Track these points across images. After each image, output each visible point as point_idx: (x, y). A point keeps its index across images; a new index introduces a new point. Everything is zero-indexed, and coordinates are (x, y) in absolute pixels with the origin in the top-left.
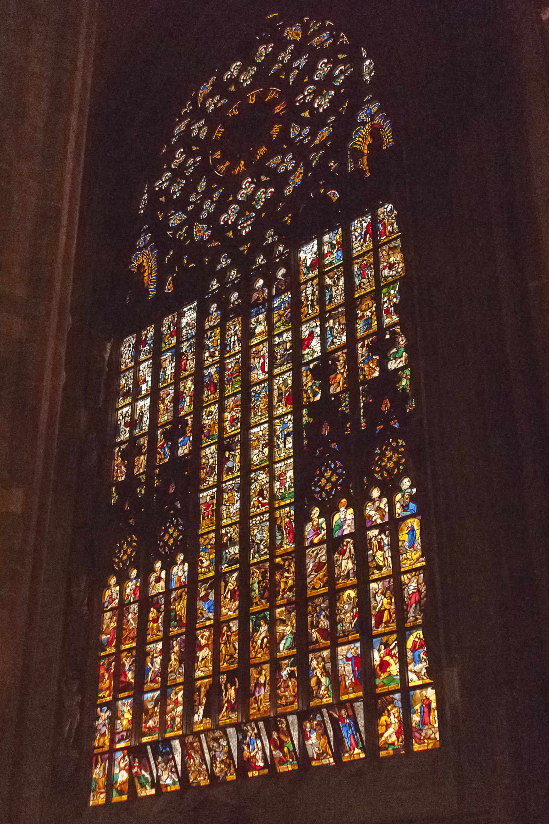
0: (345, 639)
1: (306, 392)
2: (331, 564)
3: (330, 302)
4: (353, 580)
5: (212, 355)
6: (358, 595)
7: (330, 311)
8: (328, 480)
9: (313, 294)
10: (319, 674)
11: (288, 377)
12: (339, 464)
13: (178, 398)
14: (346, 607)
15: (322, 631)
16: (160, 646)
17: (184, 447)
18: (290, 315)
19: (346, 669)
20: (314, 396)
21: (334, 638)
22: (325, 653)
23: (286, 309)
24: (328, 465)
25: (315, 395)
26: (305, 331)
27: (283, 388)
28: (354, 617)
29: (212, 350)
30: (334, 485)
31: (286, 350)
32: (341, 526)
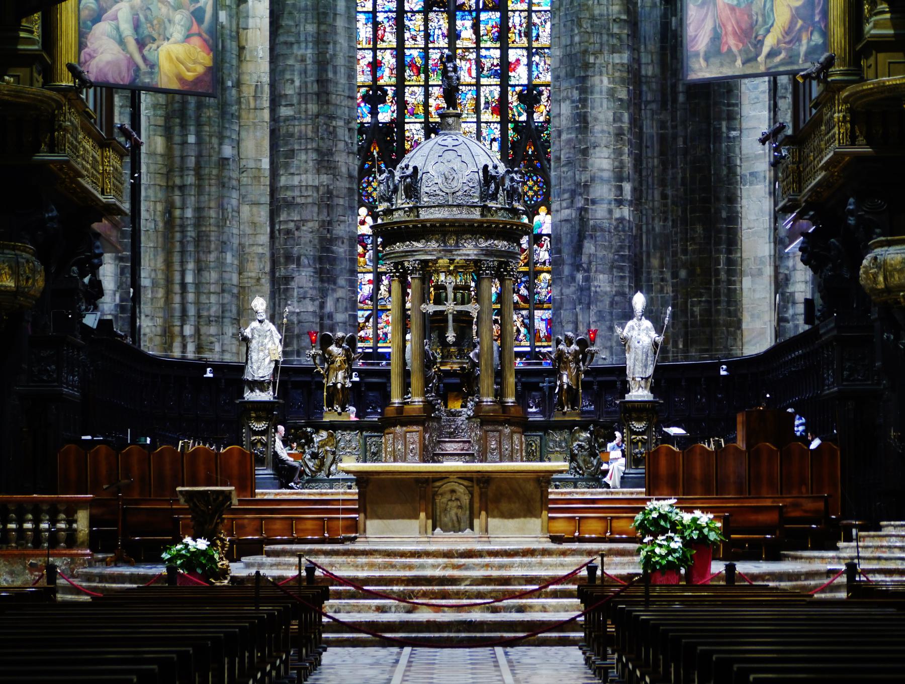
0: (540, 306)
1: (512, 109)
2: (532, 252)
3: (537, 40)
4: (548, 267)
5: (414, 38)
6: (552, 279)
7: (537, 48)
8: (531, 188)
9: (521, 25)
10: (519, 325)
11: (496, 92)
12: (540, 179)
13: (375, 65)
14: (543, 284)
15: (521, 296)
16: (370, 276)
17: (385, 114)
18: (497, 34)
19: (540, 326)
20: (519, 116)
21: (532, 303)
22: (524, 313)
23: (493, 27)
24: (532, 177)
25: (520, 115)
26: (512, 55)
27: (490, 98)
28: (548, 293)
29: (414, 33)
30: (536, 193)
31: (492, 65)
32: (540, 226)
